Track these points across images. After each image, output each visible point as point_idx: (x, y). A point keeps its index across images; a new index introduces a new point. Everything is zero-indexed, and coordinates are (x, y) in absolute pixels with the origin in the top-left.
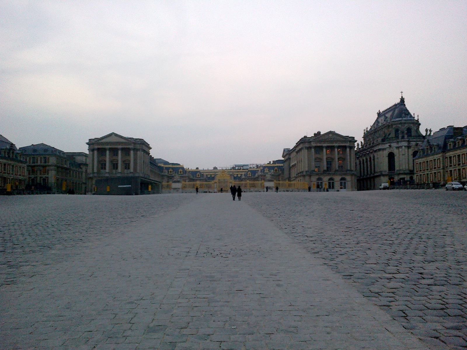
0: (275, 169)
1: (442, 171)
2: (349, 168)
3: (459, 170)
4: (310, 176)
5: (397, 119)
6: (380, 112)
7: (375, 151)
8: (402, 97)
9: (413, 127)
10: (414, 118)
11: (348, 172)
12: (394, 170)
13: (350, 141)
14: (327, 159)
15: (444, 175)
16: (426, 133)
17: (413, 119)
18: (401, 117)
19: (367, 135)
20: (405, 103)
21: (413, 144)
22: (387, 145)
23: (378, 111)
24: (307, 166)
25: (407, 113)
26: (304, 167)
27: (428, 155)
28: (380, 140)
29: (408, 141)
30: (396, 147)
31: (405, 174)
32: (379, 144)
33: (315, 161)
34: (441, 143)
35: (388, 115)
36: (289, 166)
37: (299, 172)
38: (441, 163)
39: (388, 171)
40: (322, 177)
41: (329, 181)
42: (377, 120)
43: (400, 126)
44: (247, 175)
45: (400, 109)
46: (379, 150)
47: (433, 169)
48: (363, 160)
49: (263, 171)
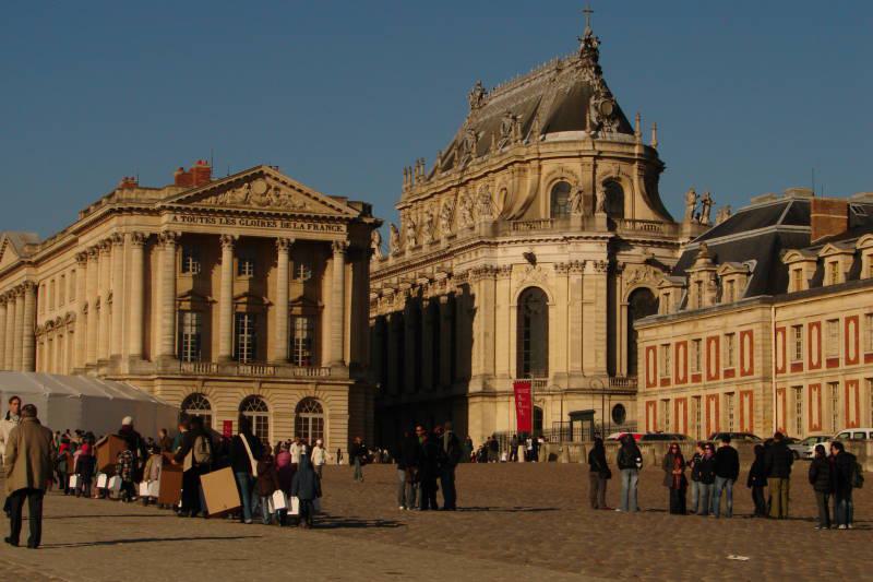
5: (563, 135)
12: (547, 375)
30: (556, 267)
31: (592, 392)
38: (758, 351)
43: (575, 165)
47: (722, 379)
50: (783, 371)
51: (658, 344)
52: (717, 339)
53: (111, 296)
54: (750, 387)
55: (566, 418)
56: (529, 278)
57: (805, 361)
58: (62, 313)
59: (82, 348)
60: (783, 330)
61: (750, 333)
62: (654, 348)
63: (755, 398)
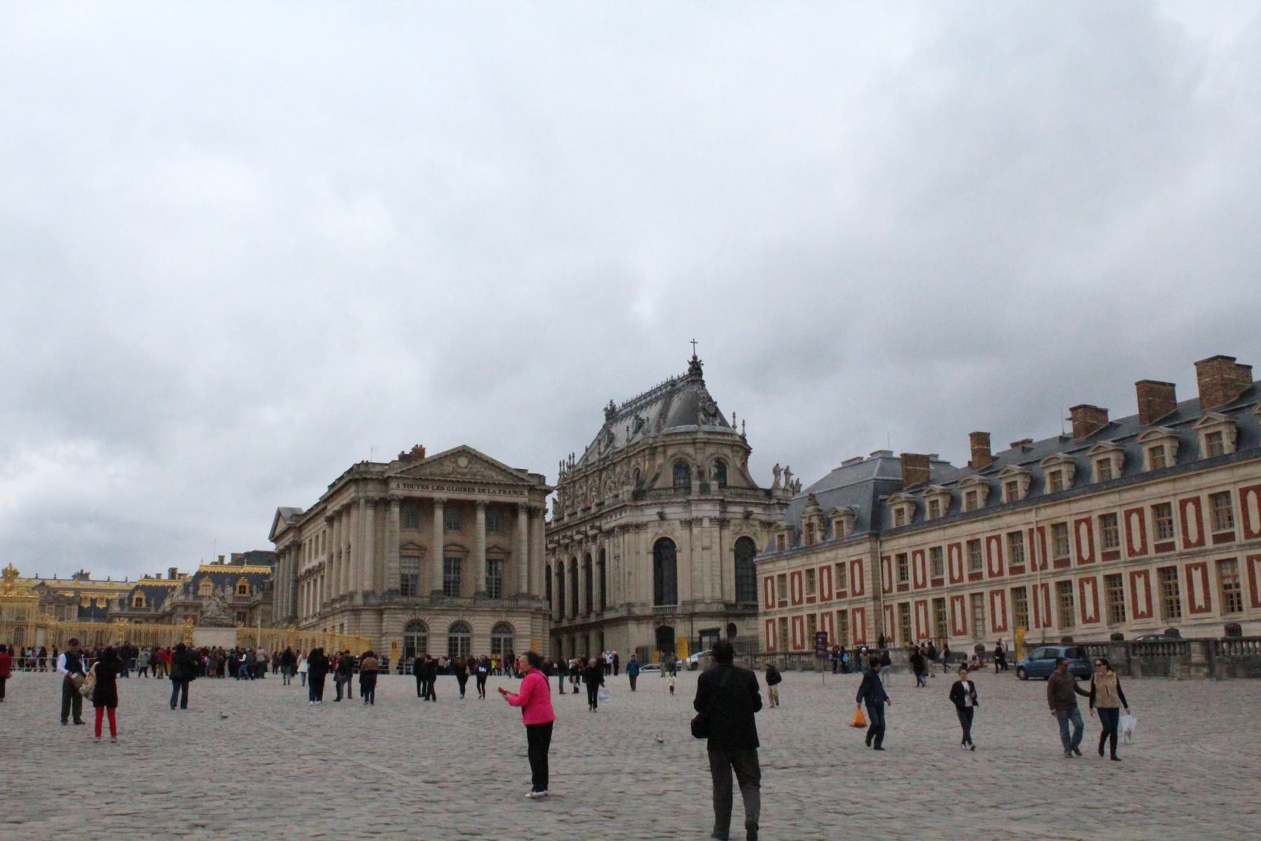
0: (238, 585)
1: (870, 606)
2: (524, 589)
3: (939, 602)
4: (380, 613)
5: (682, 428)
6: (613, 408)
7: (609, 533)
8: (695, 357)
9: (730, 455)
10: (734, 427)
11: (522, 602)
12: (676, 603)
13: (532, 489)
14: (446, 548)
15: (877, 621)
16: (777, 483)
17: (728, 430)
18: (694, 421)
19: (573, 477)
20: (704, 378)
21: (736, 511)
22: (651, 514)
23: (606, 404)
24: (368, 570)
25: (712, 412)
26: (358, 576)
27: (811, 548)
28: (626, 491)
29: (723, 504)
32: (623, 508)
33: (402, 557)
34: (863, 506)
35: (651, 413)
36: (295, 572)
37: (333, 596)
39: (652, 605)
40: (425, 617)
41: (454, 635)
42: (606, 428)
43: (690, 450)
44: (130, 599)
45: (689, 394)
46: (624, 528)
48: (561, 565)
49: (191, 588)
50: (890, 590)
51: (775, 575)
52: (829, 568)
53: (349, 547)
54: (862, 605)
55: (697, 635)
56: (661, 531)
57: (911, 582)
58: (315, 563)
59: (329, 587)
60: (888, 558)
61: (860, 562)
62: (772, 578)
63: (867, 613)
